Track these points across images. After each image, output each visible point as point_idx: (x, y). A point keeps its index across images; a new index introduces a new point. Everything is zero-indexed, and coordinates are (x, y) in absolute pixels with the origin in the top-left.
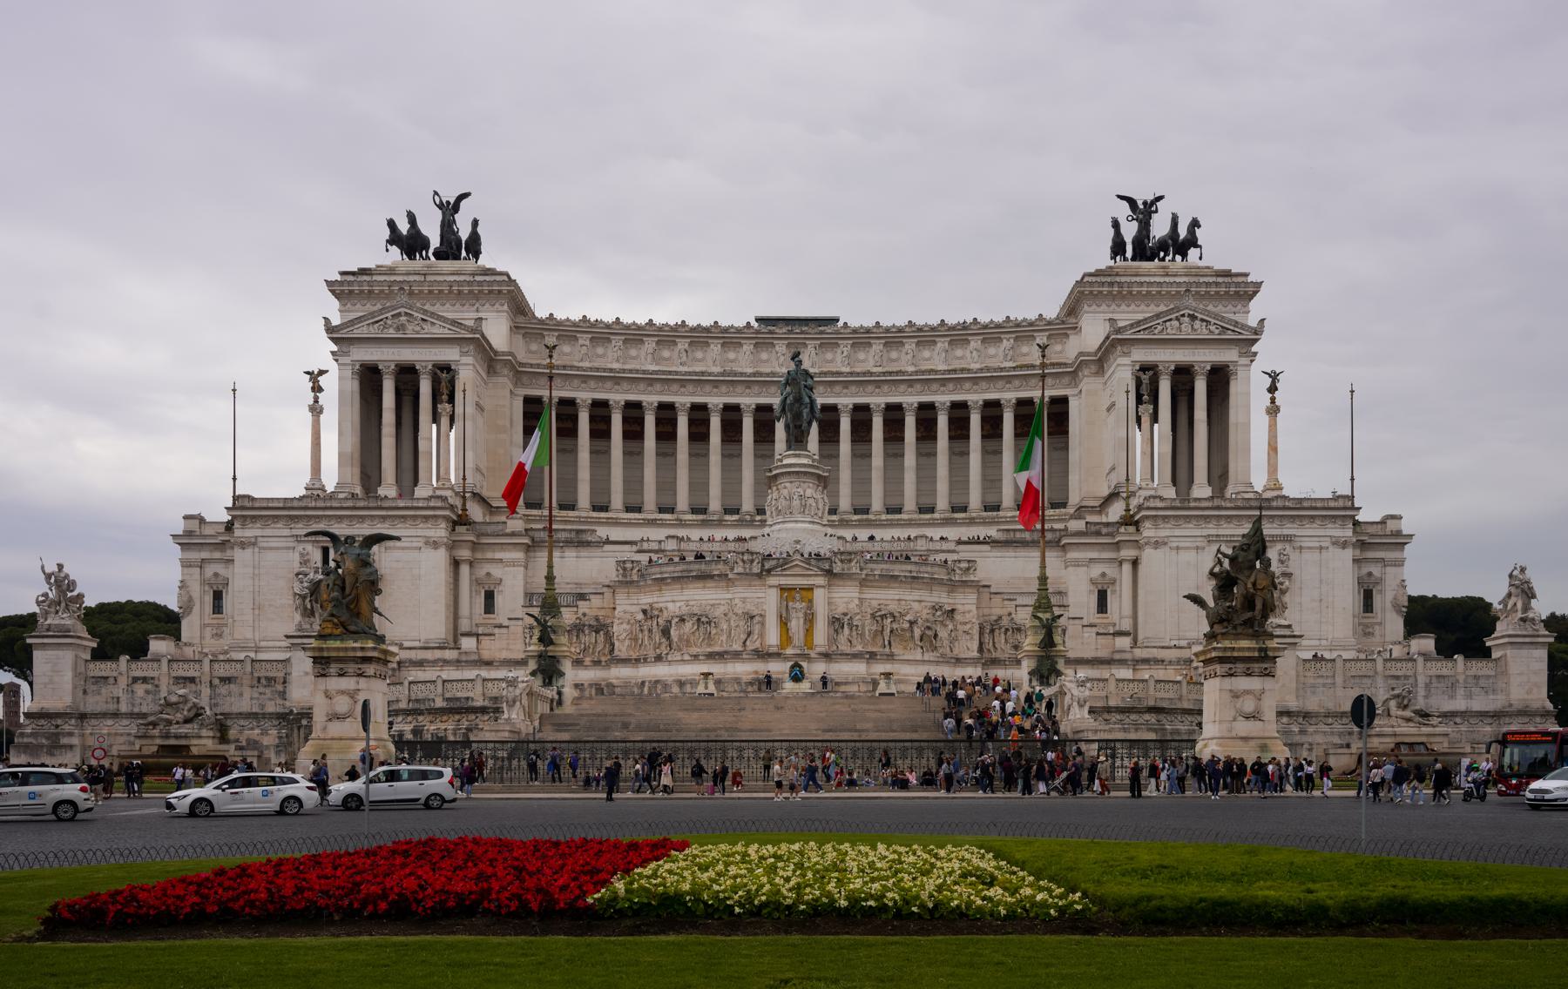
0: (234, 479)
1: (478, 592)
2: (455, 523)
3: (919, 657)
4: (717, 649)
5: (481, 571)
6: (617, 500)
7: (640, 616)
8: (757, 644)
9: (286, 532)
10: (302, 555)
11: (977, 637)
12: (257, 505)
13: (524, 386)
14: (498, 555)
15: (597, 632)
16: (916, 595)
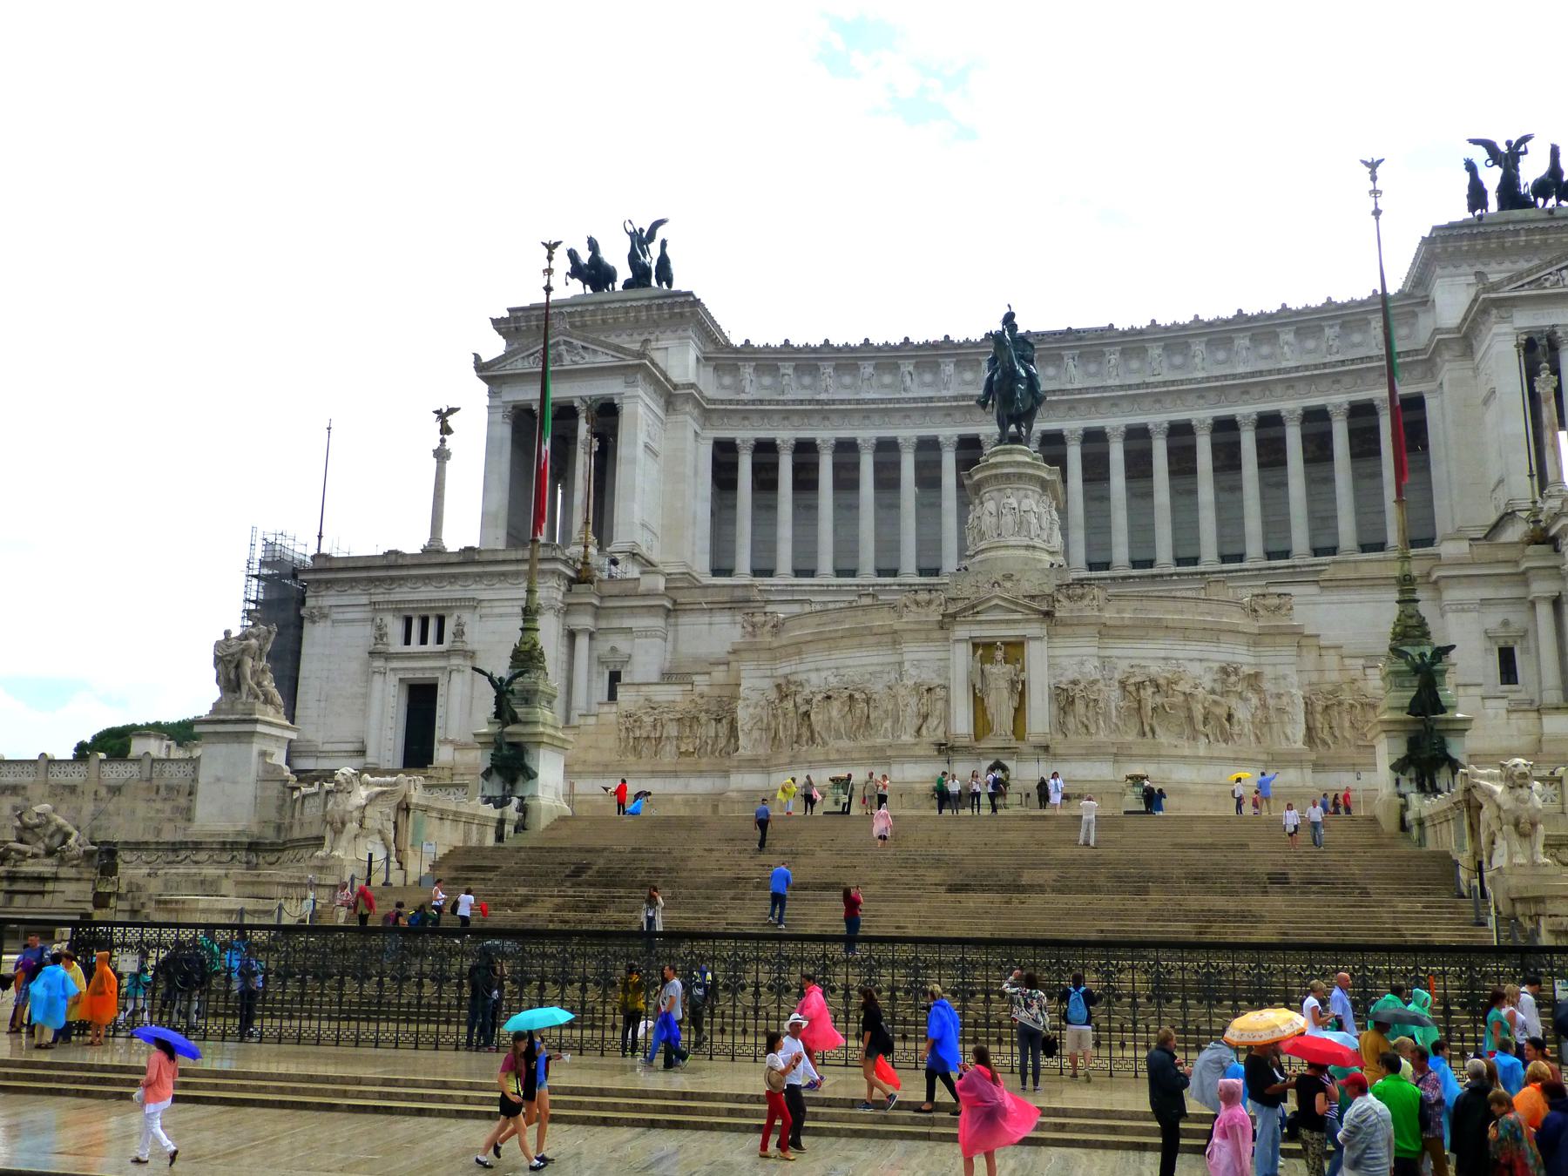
0: (320, 537)
1: (600, 674)
2: (572, 581)
3: (1202, 753)
4: (879, 741)
5: (603, 646)
6: (826, 563)
7: (773, 695)
8: (939, 735)
9: (364, 600)
10: (379, 628)
11: (1301, 718)
12: (335, 565)
13: (713, 427)
14: (627, 623)
15: (719, 721)
16: (1193, 649)
